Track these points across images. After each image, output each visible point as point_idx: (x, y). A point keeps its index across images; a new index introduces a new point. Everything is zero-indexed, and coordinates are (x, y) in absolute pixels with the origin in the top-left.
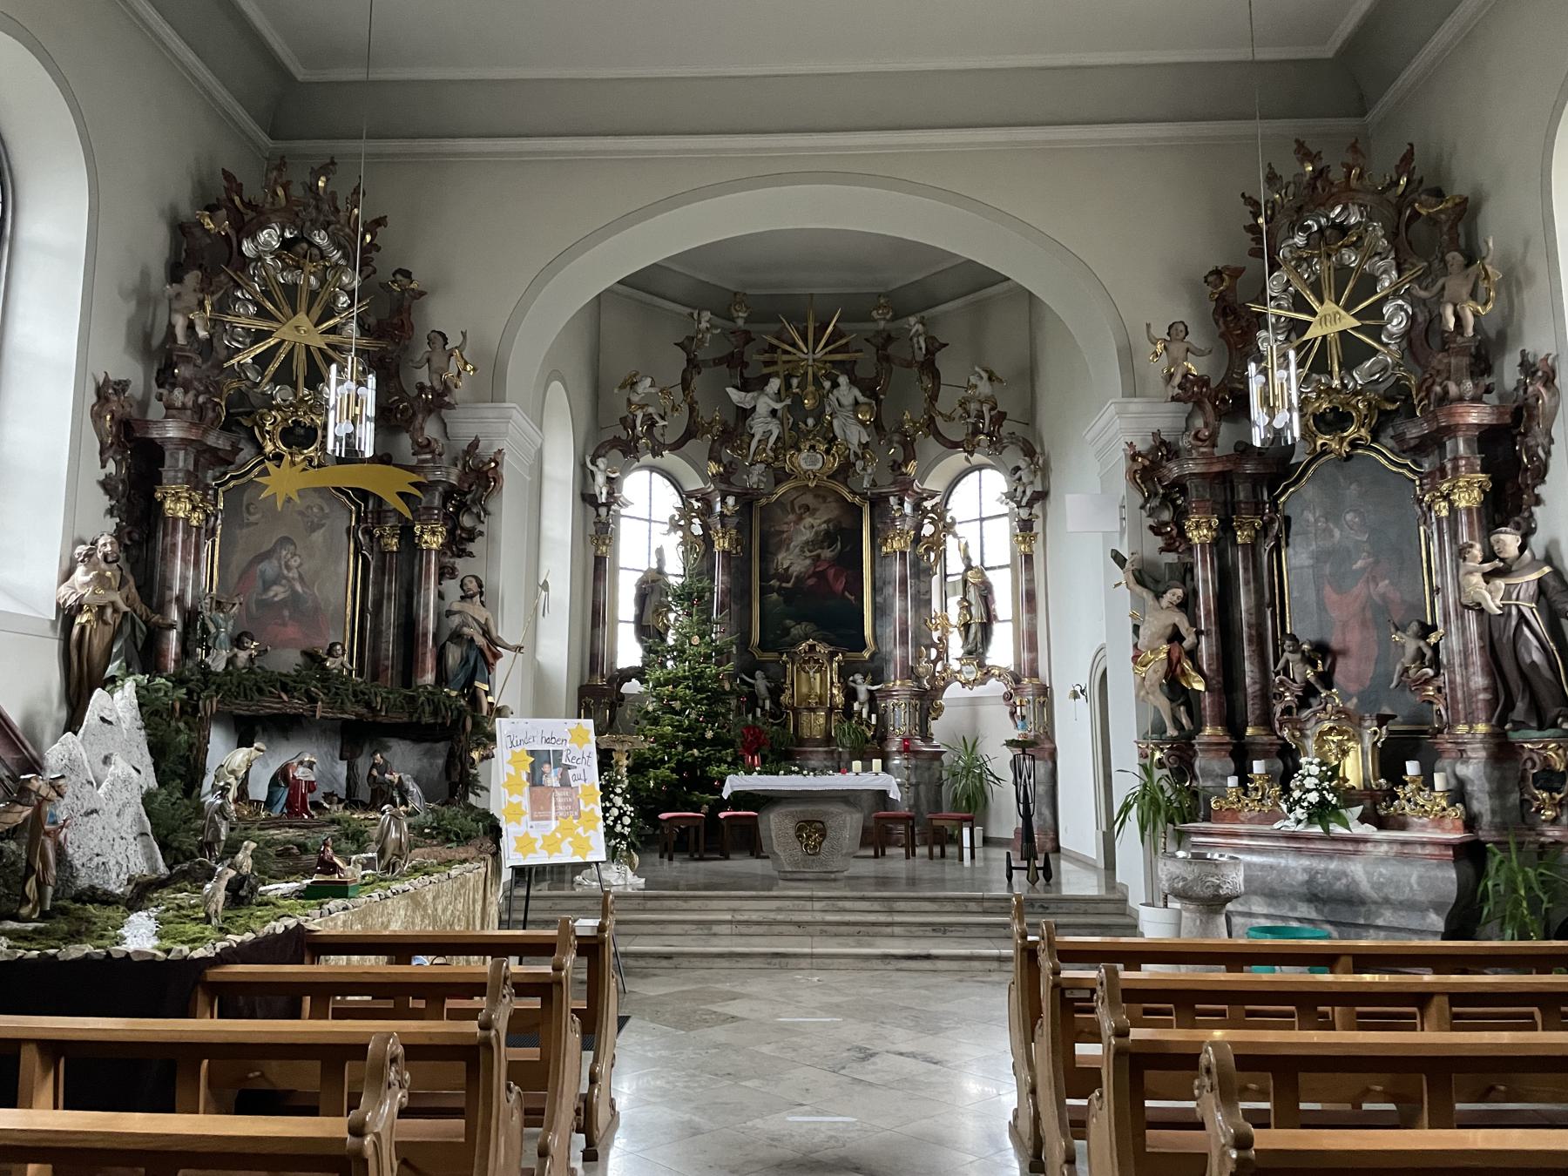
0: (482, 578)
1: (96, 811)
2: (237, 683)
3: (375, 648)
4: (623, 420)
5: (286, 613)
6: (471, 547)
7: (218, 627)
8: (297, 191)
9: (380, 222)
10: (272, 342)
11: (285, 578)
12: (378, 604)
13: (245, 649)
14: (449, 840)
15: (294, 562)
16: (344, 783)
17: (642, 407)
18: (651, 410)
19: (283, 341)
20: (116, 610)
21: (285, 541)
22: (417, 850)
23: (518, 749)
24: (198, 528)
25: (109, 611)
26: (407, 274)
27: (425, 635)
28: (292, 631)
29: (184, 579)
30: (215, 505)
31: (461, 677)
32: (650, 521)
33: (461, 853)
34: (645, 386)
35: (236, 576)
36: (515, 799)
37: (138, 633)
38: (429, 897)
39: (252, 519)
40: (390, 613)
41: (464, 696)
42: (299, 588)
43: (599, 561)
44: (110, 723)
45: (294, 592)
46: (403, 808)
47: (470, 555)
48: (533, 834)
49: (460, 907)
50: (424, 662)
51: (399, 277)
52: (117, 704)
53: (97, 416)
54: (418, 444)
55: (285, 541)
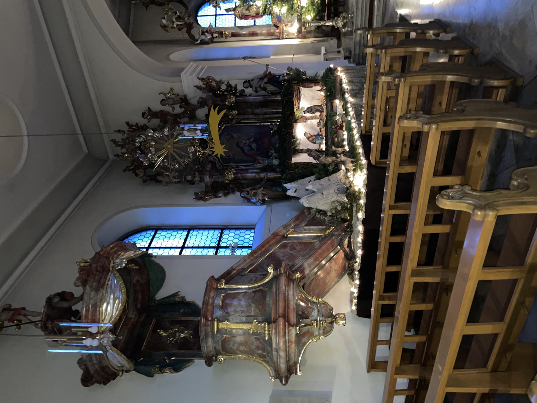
0: (243, 81)
4: (180, 30)
6: (233, 85)
8: (124, 150)
9: (127, 123)
10: (175, 154)
15: (244, 142)
17: (173, 23)
18: (174, 20)
19: (174, 151)
21: (237, 145)
24: (236, 170)
25: (264, 192)
26: (143, 114)
29: (252, 173)
30: (229, 166)
32: (216, 15)
34: (164, 21)
39: (232, 155)
42: (252, 140)
43: (234, 35)
45: (253, 141)
47: (236, 85)
51: (145, 116)
52: (291, 188)
53: (206, 200)
54: (200, 106)
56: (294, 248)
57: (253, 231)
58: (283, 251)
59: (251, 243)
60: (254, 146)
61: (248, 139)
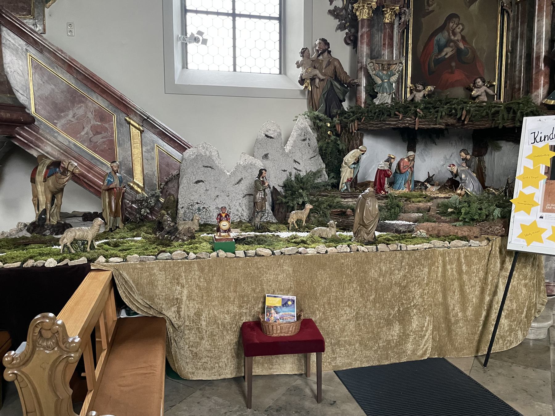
1: (202, 181)
5: (453, 64)
7: (382, 80)
12: (514, 44)
13: (420, 91)
14: (457, 220)
15: (458, 30)
21: (451, 17)
23: (540, 145)
24: (392, 24)
27: (538, 58)
28: (458, 75)
36: (528, 191)
37: (337, 91)
39: (431, 9)
40: (521, 49)
42: (461, 46)
44: (271, 137)
45: (459, 50)
48: (541, 224)
50: (538, 81)
55: (451, 17)
56: (98, 133)
58: (90, 115)
59: (245, 69)
60: (448, 52)
61: (463, 38)
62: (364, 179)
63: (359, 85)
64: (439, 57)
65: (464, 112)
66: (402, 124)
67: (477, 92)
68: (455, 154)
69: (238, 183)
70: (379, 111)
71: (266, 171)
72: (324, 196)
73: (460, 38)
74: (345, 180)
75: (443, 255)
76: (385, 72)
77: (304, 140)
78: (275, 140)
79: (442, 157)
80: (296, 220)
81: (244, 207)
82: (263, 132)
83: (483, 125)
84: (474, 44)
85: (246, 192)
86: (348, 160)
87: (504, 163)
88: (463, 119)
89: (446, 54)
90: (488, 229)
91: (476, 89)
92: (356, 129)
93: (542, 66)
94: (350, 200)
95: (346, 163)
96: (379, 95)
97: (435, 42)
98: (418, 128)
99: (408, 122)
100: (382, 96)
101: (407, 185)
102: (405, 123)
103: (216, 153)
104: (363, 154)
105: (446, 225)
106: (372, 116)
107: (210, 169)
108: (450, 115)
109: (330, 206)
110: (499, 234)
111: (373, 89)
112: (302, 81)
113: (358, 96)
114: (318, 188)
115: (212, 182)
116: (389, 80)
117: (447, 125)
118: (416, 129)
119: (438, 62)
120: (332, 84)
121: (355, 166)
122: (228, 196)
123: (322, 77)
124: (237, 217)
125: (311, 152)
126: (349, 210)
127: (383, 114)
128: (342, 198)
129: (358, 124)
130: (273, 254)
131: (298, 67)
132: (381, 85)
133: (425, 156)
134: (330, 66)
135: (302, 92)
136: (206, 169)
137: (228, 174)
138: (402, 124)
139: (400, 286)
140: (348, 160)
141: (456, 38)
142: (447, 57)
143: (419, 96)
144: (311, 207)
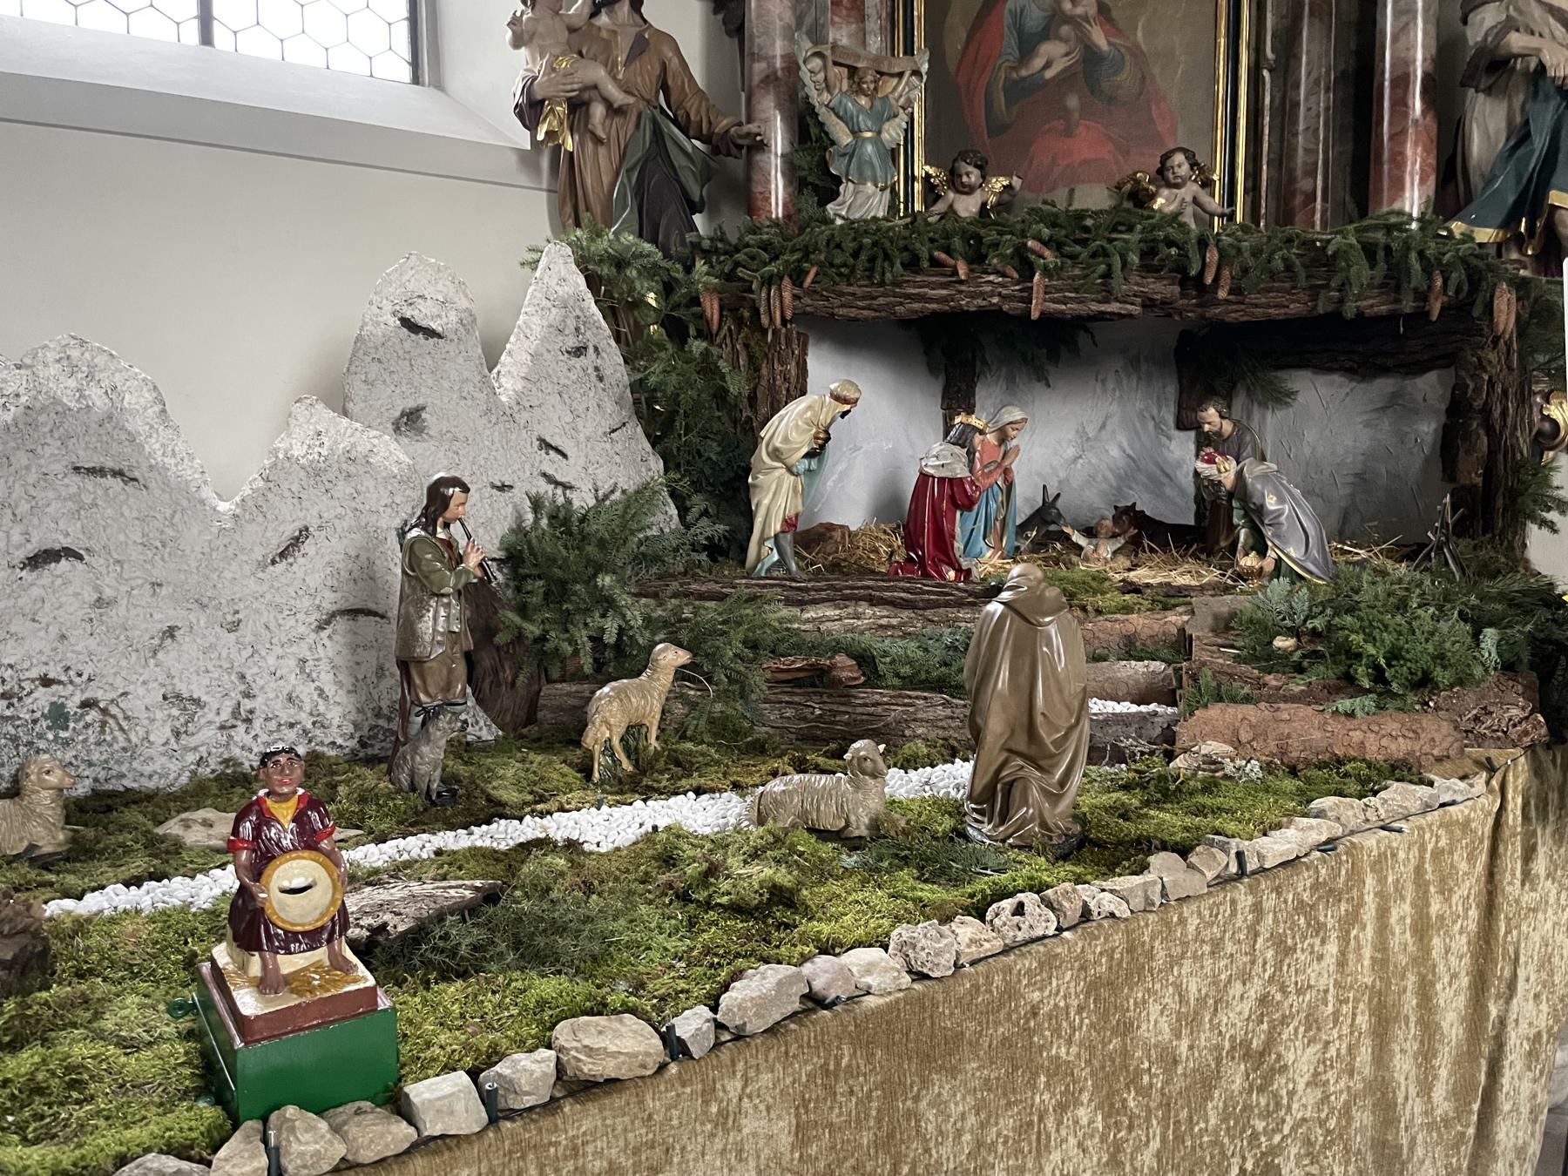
1: (70, 553)
2: (872, 249)
3: (1283, 157)
5: (1073, 102)
7: (855, 132)
11: (1069, 20)
13: (969, 190)
14: (1348, 684)
16: (1192, 490)
20: (614, 111)
22: (1215, 711)
25: (598, 111)
27: (1402, 82)
31: (1507, 189)
33: (1379, 733)
35: (964, 36)
37: (679, 161)
38: (1061, 991)
41: (1519, 241)
42: (1100, 39)
44: (430, 333)
46: (1249, 561)
49: (1322, 974)
50: (1399, 161)
57: (406, 73)
59: (258, 46)
62: (811, 514)
63: (761, 146)
64: (1024, 73)
65: (1212, 256)
66: (973, 296)
67: (1169, 201)
68: (1116, 420)
69: (282, 555)
70: (875, 244)
71: (466, 490)
72: (702, 596)
73: (1093, 11)
74: (776, 526)
75: (1380, 863)
76: (863, 101)
77: (579, 351)
78: (451, 348)
79: (1068, 432)
80: (622, 730)
81: (326, 680)
82: (388, 307)
83: (1277, 306)
84: (1140, 34)
85: (329, 601)
86: (786, 440)
87: (1307, 451)
88: (1209, 281)
89: (1048, 65)
90: (1476, 719)
91: (1165, 192)
92: (789, 314)
93: (1418, 105)
94: (831, 613)
95: (776, 454)
96: (847, 189)
97: (1007, 20)
98: (1042, 313)
99: (992, 289)
100: (856, 193)
101: (991, 540)
102: (983, 295)
103: (149, 396)
104: (844, 415)
105: (1305, 711)
106: (845, 265)
107: (116, 484)
108: (1147, 268)
109: (754, 645)
110: (1527, 741)
111: (824, 165)
112: (530, 110)
113: (757, 189)
114: (657, 559)
115: (135, 553)
116: (879, 133)
117: (1149, 304)
118: (1035, 315)
119: (1020, 90)
120: (657, 133)
121: (814, 464)
122: (234, 627)
123: (619, 97)
124: (291, 735)
125: (609, 406)
126: (841, 659)
127: (887, 257)
128: (789, 602)
129: (796, 297)
130: (676, 1048)
131: (517, 42)
132: (850, 153)
133: (1256, 406)
134: (645, 57)
135: (528, 160)
136: (90, 483)
137: (223, 507)
138: (973, 296)
139: (1247, 1055)
140: (786, 440)
141: (1079, 10)
142: (1049, 74)
143: (967, 207)
144: (683, 657)
